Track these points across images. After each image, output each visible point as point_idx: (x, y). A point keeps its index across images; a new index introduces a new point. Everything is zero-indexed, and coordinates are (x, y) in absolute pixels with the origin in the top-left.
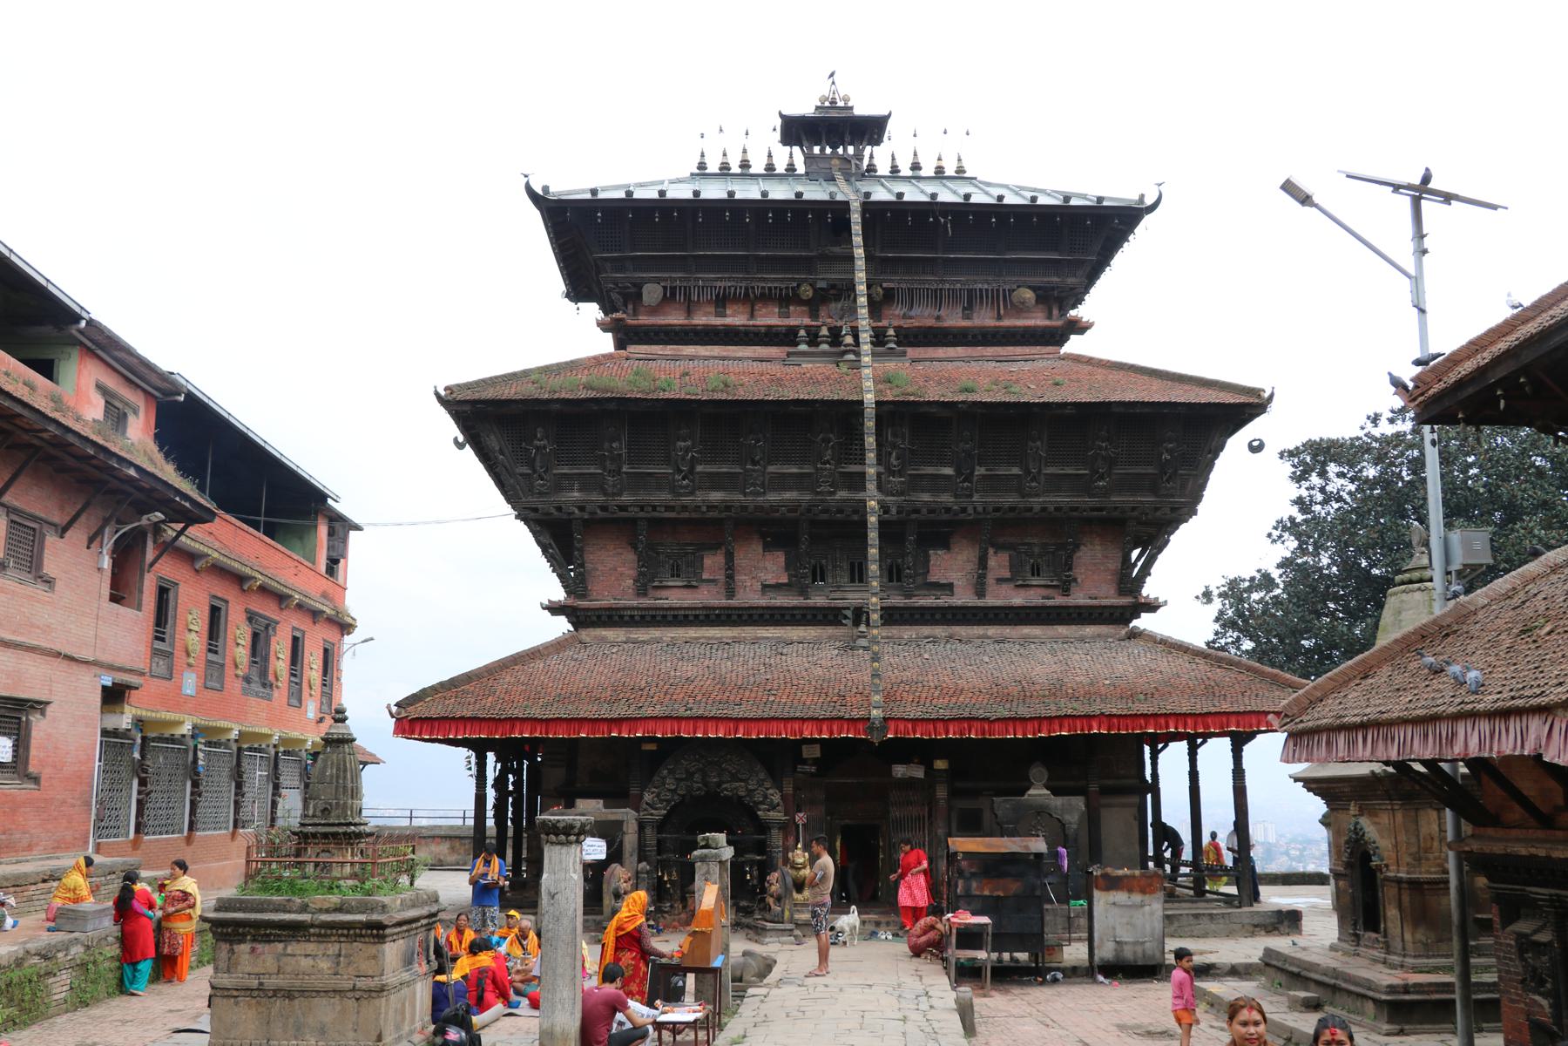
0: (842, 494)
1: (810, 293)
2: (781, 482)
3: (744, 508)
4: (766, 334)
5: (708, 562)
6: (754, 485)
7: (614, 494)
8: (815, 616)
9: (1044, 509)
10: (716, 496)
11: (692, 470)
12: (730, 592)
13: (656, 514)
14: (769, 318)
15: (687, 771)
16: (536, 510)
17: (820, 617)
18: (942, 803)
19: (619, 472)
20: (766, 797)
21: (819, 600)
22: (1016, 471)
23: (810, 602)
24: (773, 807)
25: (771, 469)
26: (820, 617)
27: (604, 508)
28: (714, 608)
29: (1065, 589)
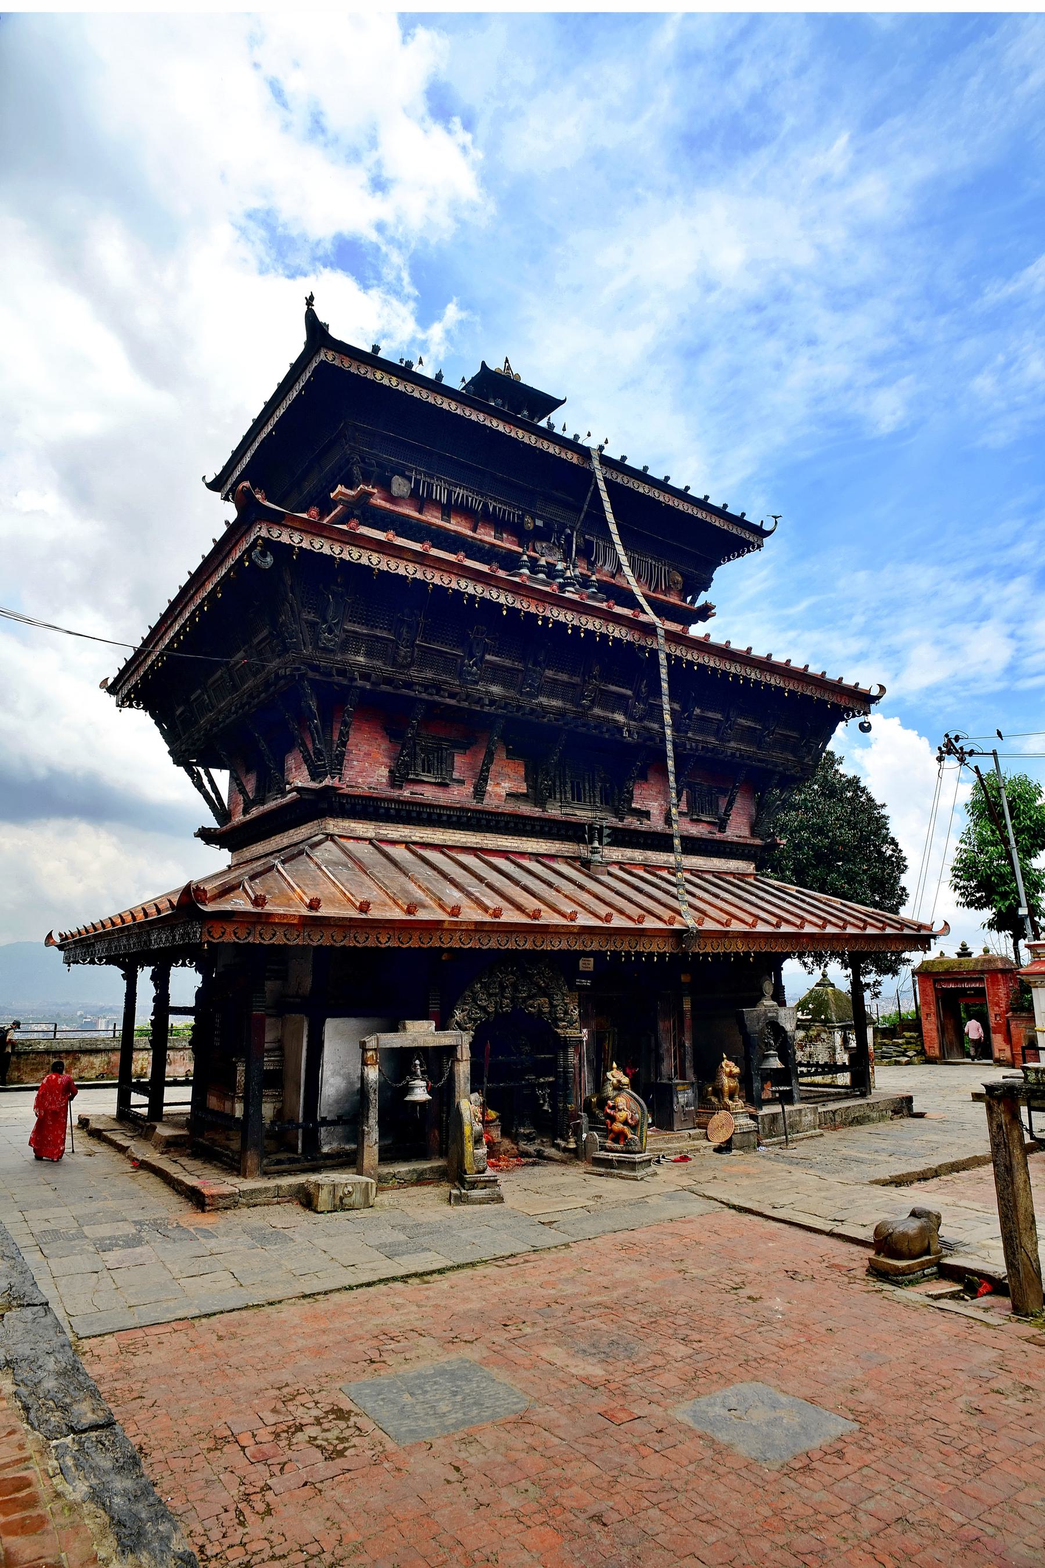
0: (597, 711)
1: (531, 526)
2: (553, 689)
3: (519, 708)
4: (489, 551)
5: (459, 760)
6: (530, 686)
7: (403, 667)
8: (542, 827)
9: (733, 755)
10: (495, 689)
11: (483, 656)
12: (479, 793)
13: (437, 698)
14: (486, 536)
15: (501, 984)
16: (316, 668)
17: (555, 831)
18: (688, 1015)
19: (413, 645)
20: (566, 1013)
21: (554, 812)
22: (719, 716)
23: (545, 815)
24: (571, 1024)
25: (549, 673)
26: (555, 831)
27: (389, 681)
28: (469, 810)
29: (722, 828)
